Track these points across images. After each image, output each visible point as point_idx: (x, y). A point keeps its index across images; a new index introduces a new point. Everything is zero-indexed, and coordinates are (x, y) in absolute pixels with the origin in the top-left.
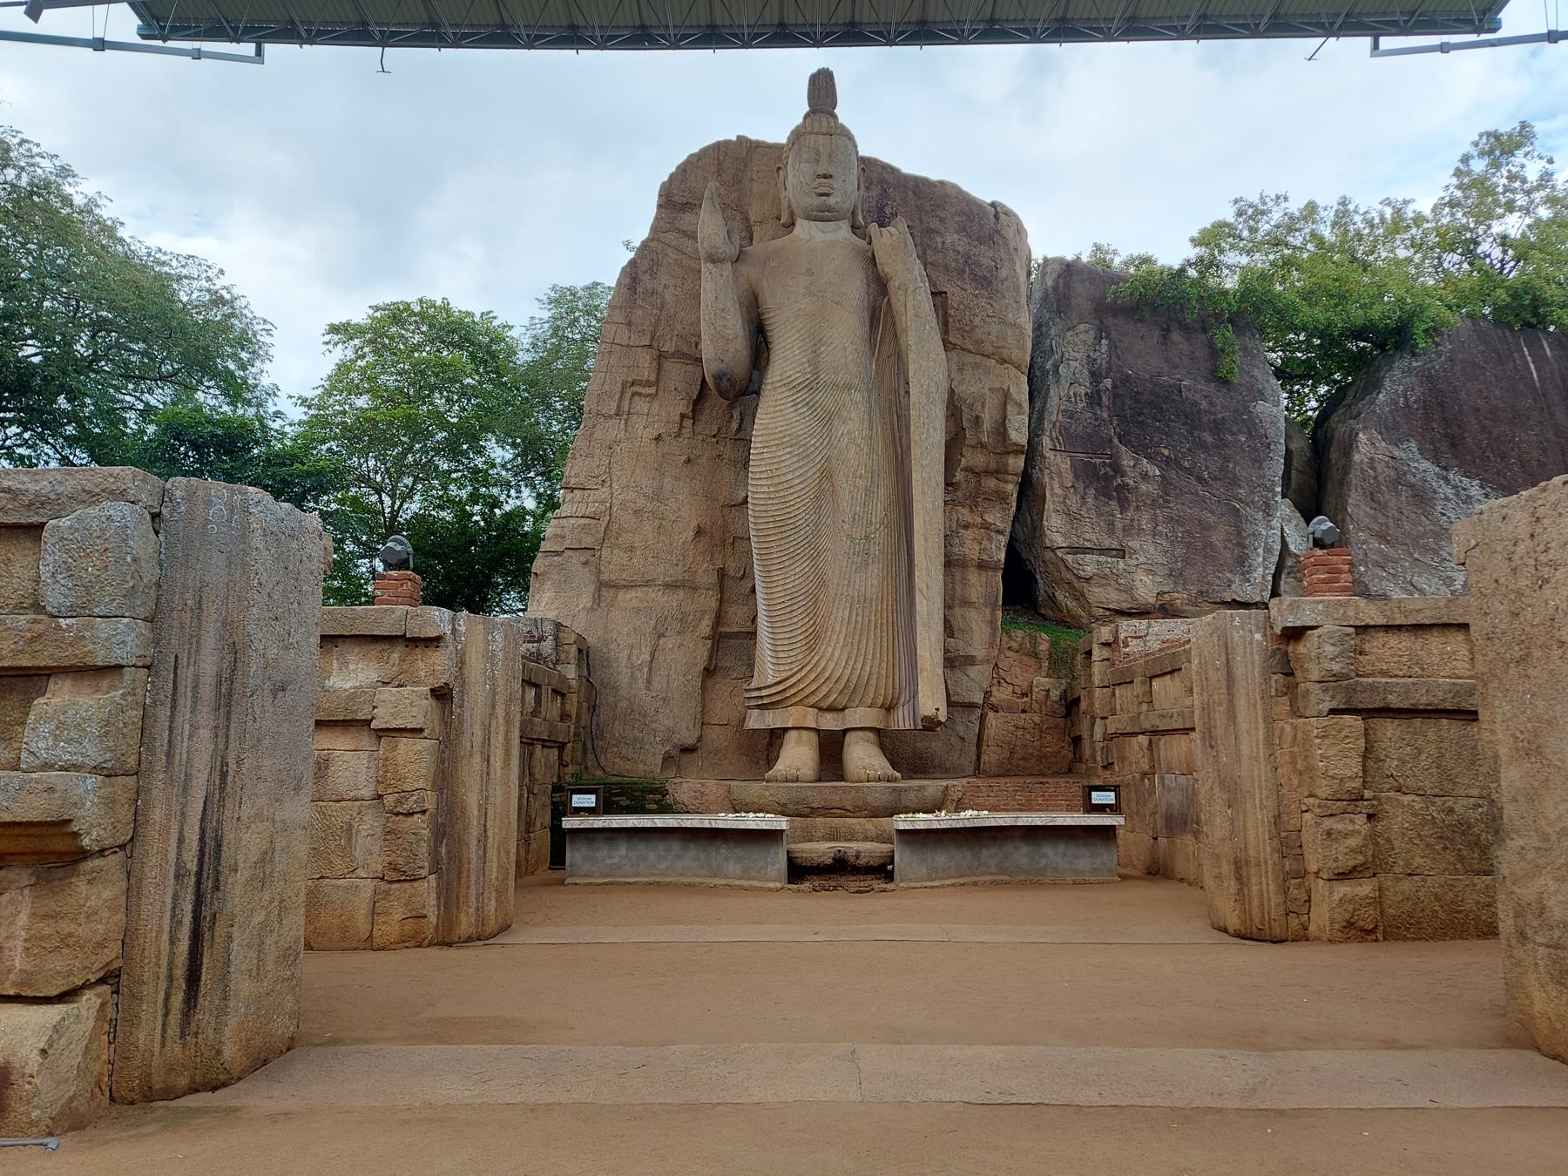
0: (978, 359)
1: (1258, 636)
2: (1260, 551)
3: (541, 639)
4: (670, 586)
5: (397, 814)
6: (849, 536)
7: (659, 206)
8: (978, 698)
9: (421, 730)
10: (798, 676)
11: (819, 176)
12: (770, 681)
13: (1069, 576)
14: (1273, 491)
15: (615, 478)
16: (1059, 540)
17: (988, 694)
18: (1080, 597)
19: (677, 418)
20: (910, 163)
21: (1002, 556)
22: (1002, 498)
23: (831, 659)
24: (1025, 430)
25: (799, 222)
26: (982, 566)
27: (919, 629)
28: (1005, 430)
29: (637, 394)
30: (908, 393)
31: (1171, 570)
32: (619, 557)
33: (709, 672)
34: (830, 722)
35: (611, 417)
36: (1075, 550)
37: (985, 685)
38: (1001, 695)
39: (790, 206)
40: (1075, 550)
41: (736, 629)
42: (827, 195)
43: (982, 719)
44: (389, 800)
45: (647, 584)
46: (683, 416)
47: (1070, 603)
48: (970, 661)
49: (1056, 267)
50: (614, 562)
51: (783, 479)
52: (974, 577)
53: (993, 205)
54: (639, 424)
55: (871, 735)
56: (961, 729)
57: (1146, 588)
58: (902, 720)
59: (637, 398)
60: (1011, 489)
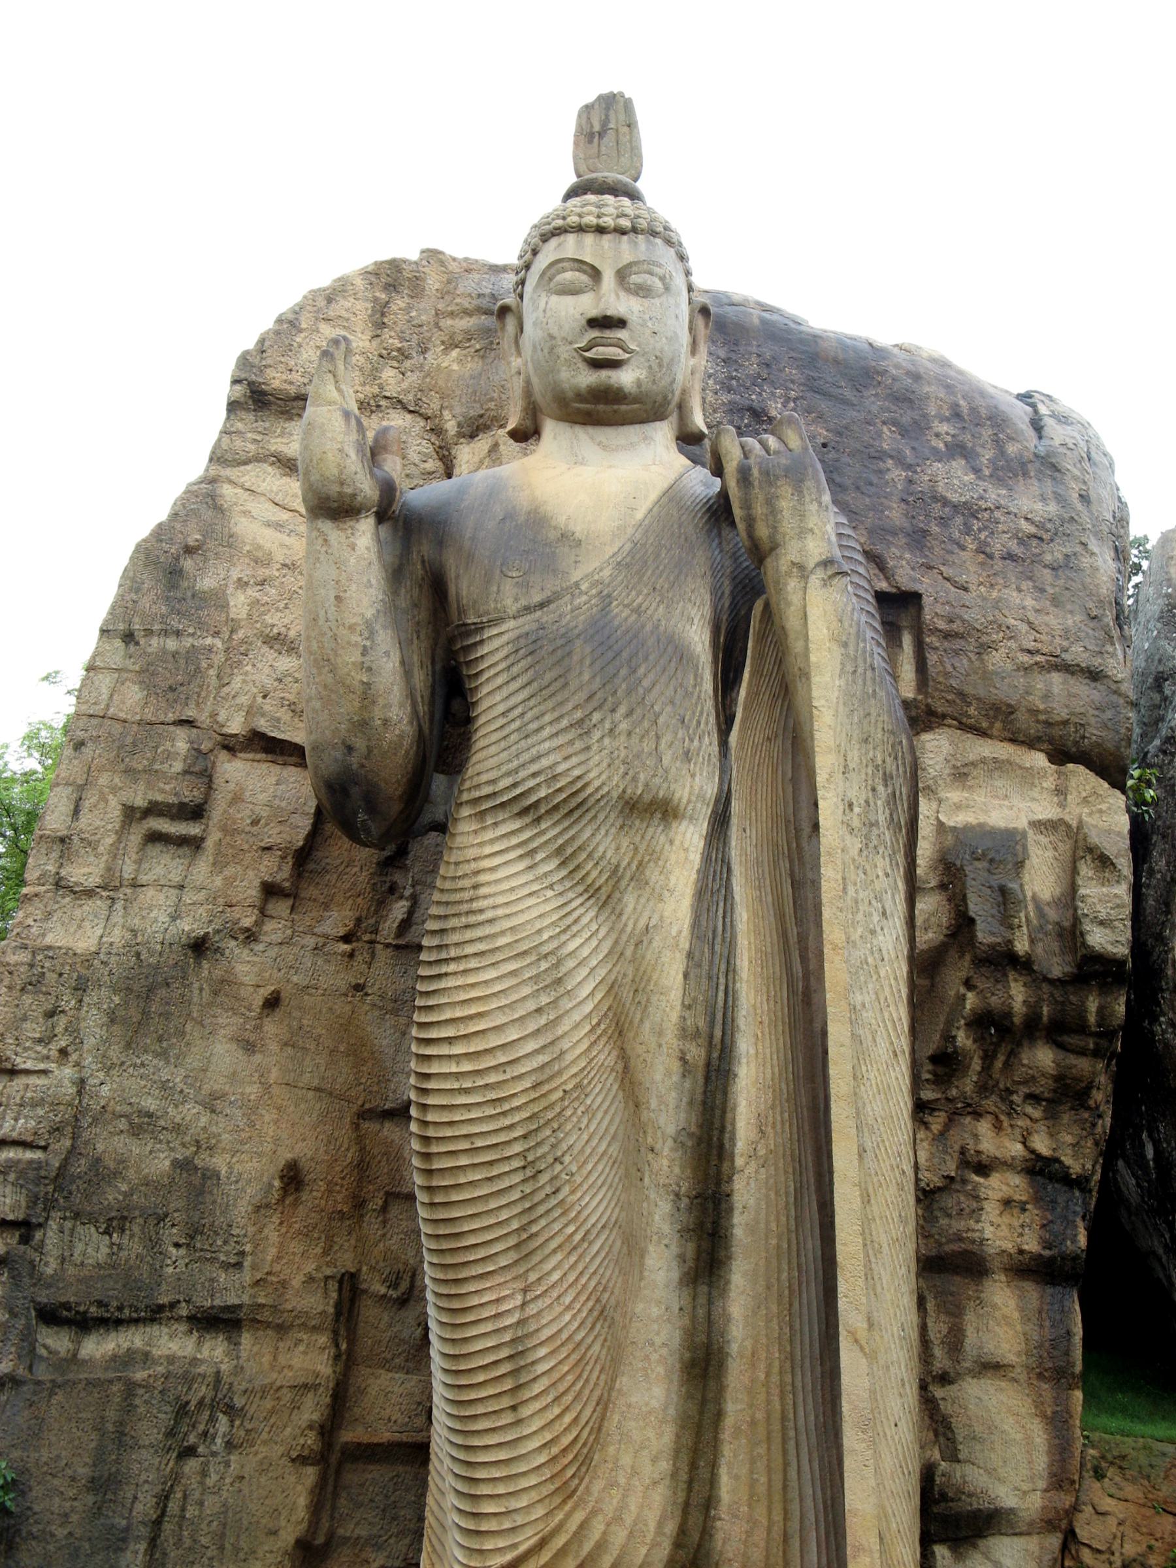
7: (233, 406)
11: (593, 323)
20: (834, 303)
21: (1082, 1240)
25: (550, 428)
27: (852, 1439)
28: (1076, 921)
29: (155, 838)
30: (816, 827)
35: (90, 893)
39: (528, 393)
41: (385, 1435)
42: (614, 364)
46: (270, 890)
51: (494, 1041)
59: (155, 850)
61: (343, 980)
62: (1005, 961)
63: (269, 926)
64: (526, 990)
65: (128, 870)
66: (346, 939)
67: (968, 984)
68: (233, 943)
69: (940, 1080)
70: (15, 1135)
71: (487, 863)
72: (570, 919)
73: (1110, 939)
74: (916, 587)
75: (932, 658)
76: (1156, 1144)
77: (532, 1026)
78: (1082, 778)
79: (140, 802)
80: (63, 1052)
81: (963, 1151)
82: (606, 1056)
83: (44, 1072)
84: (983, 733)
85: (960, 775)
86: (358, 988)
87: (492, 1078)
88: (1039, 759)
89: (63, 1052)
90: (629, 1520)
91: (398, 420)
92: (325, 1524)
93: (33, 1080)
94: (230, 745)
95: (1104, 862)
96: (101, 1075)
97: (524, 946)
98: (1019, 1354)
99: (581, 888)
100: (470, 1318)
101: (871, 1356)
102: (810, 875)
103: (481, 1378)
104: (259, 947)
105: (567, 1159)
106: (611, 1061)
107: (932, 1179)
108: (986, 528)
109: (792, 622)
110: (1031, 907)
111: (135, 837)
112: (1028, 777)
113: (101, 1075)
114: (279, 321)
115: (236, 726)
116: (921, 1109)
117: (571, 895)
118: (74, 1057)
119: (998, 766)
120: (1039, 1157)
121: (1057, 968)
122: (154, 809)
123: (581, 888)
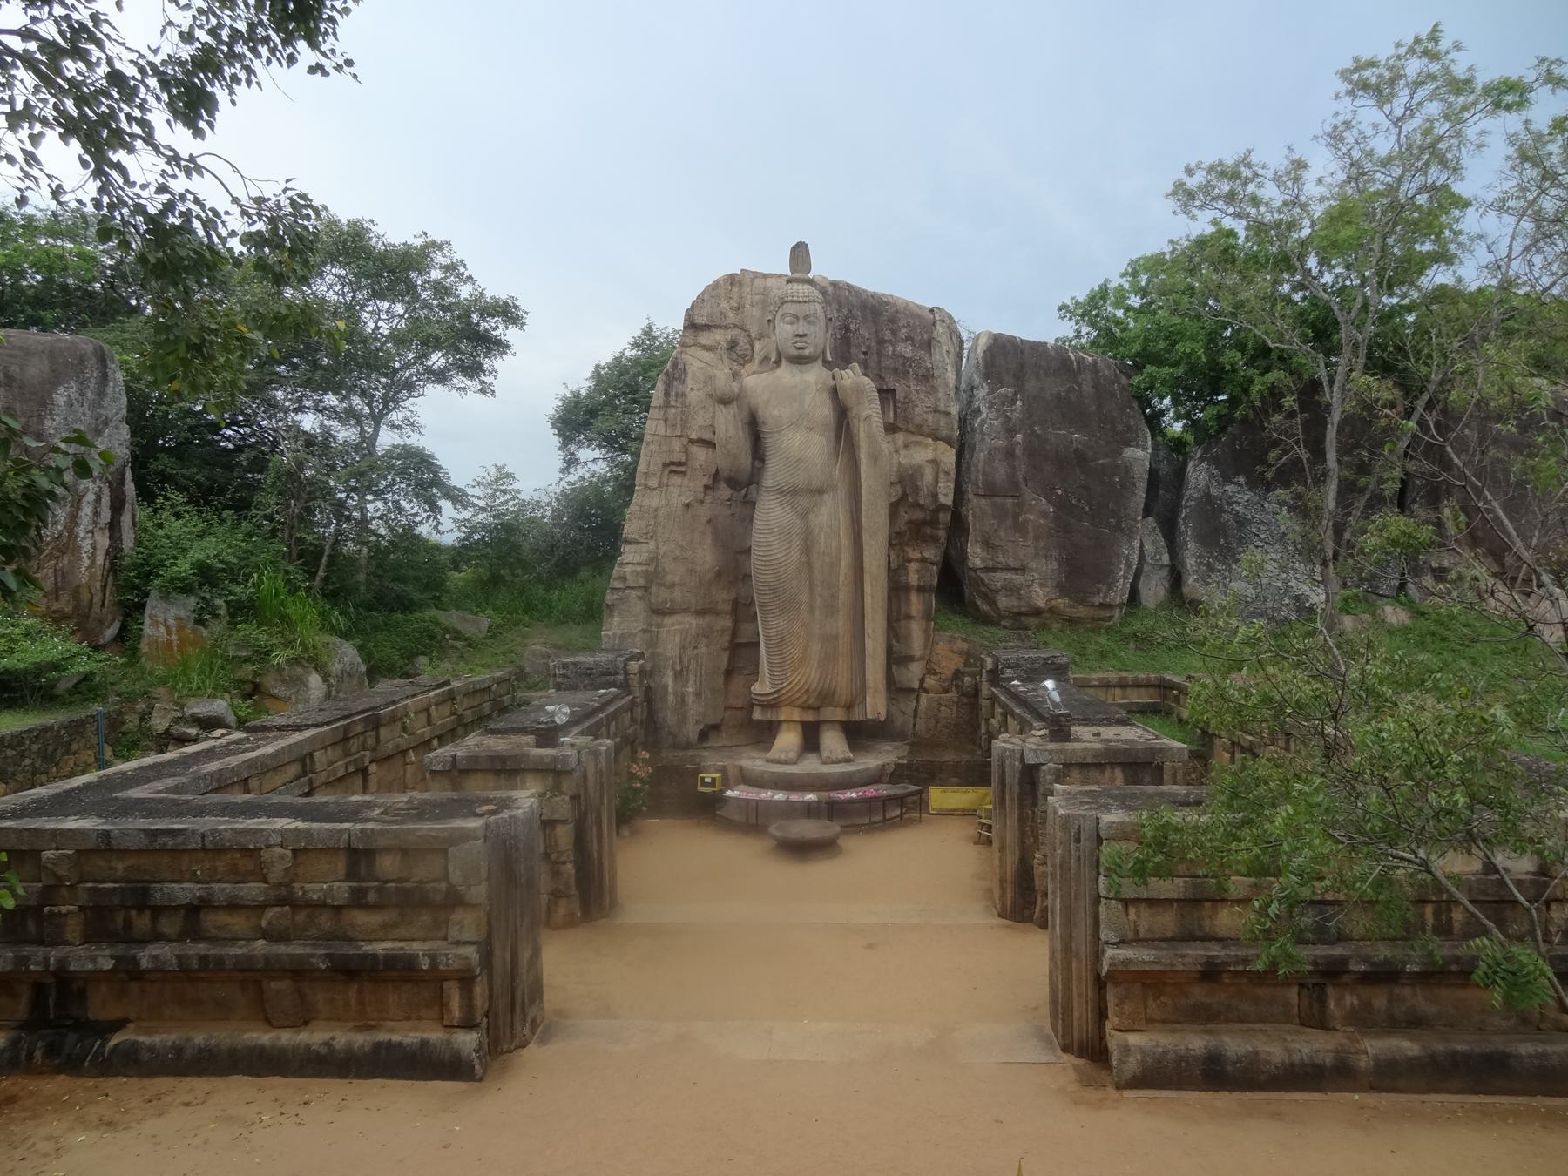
0: (920, 438)
3: (617, 673)
4: (700, 613)
8: (916, 685)
12: (768, 690)
14: (1135, 520)
16: (978, 562)
17: (922, 681)
18: (993, 603)
26: (920, 589)
29: (672, 471)
32: (664, 593)
33: (729, 673)
34: (810, 717)
36: (988, 570)
38: (930, 682)
40: (988, 570)
44: (553, 856)
45: (684, 611)
46: (706, 487)
47: (986, 608)
48: (911, 659)
49: (983, 343)
50: (660, 595)
53: (932, 310)
54: (675, 491)
55: (837, 726)
57: (1040, 597)
58: (857, 716)
60: (942, 533)
61: (729, 512)
62: (917, 505)
69: (897, 541)
78: (942, 445)
85: (906, 446)
88: (930, 440)
91: (736, 332)
95: (947, 474)
112: (926, 446)
115: (694, 436)
116: (891, 545)
119: (918, 443)
122: (672, 463)
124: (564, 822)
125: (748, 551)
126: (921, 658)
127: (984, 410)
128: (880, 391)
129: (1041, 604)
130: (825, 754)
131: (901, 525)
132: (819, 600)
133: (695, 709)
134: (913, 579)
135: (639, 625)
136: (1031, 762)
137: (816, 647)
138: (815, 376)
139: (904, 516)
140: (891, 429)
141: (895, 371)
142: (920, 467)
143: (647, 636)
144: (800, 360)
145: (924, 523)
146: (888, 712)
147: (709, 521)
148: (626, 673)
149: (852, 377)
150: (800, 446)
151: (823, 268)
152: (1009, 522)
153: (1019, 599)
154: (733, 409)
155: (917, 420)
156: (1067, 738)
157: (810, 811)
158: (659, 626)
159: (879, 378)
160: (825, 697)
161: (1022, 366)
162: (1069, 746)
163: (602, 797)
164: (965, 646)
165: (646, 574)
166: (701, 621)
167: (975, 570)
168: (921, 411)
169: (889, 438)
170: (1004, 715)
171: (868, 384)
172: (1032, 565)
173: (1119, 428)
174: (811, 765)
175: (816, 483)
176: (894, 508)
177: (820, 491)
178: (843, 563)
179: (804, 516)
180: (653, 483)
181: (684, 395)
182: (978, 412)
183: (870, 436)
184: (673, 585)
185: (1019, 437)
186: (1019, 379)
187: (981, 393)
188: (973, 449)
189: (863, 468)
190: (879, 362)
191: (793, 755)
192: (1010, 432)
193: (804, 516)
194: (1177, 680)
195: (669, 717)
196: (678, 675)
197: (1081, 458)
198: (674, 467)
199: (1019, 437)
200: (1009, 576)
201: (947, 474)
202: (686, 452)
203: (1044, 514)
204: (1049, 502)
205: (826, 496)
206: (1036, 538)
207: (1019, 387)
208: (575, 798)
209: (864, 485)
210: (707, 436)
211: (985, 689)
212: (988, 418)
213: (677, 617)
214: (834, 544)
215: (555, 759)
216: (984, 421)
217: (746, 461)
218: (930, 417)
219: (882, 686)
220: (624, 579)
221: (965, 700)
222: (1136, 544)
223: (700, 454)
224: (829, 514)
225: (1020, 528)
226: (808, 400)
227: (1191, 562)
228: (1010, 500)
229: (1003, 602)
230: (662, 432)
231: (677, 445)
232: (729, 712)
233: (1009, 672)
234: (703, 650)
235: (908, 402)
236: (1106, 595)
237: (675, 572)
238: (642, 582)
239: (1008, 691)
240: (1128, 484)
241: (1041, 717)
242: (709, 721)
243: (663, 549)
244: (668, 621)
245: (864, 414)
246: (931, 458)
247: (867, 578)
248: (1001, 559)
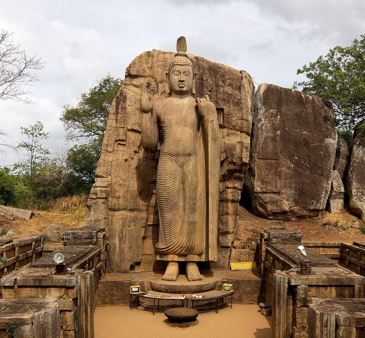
0: (234, 131)
1: (286, 285)
2: (324, 192)
3: (92, 238)
4: (132, 210)
5: (66, 331)
6: (189, 203)
8: (230, 245)
9: (71, 310)
10: (172, 246)
13: (261, 202)
15: (113, 173)
17: (233, 243)
18: (265, 208)
19: (133, 153)
21: (240, 197)
22: (240, 179)
23: (182, 241)
24: (248, 159)
26: (233, 201)
28: (242, 158)
29: (119, 144)
31: (295, 199)
32: (115, 201)
34: (182, 259)
35: (111, 152)
37: (232, 241)
38: (236, 243)
43: (231, 251)
44: (64, 327)
45: (124, 209)
46: (135, 152)
47: (262, 210)
50: (112, 201)
52: (230, 205)
56: (224, 255)
57: (286, 206)
59: (119, 146)
61: (145, 164)
63: (135, 157)
64: (171, 179)
65: (116, 148)
66: (146, 158)
67: (227, 166)
68: (131, 159)
69: (224, 178)
70: (104, 186)
71: (166, 161)
72: (177, 170)
73: (246, 160)
74: (224, 108)
75: (225, 118)
76: (251, 180)
77: (172, 183)
79: (117, 139)
80: (109, 174)
81: (226, 186)
82: (181, 186)
83: (107, 177)
84: (231, 129)
86: (147, 165)
87: (167, 190)
89: (109, 174)
90: (183, 241)
92: (146, 234)
93: (105, 178)
94: (129, 130)
96: (114, 178)
97: (171, 173)
98: (231, 212)
99: (178, 165)
100: (165, 218)
101: (213, 224)
102: (207, 159)
103: (166, 225)
104: (134, 160)
105: (176, 199)
106: (182, 187)
107: (221, 190)
108: (234, 98)
109: (206, 127)
110: (236, 155)
111: (116, 144)
112: (237, 135)
113: (114, 178)
114: (132, 62)
115: (129, 128)
117: (177, 166)
118: (111, 175)
119: (233, 134)
120: (235, 187)
121: (240, 163)
122: (119, 140)
123: (178, 165)
124: (70, 311)
125: (155, 182)
126: (233, 233)
127: (263, 119)
128: (217, 109)
129: (287, 209)
130: (189, 277)
131: (224, 171)
132: (188, 205)
133: (128, 255)
134: (230, 197)
135: (101, 216)
136: (293, 284)
137: (186, 227)
138: (188, 101)
139: (226, 167)
140: (221, 127)
141: (224, 99)
142: (234, 145)
143: (106, 220)
144: (181, 94)
145: (235, 171)
146: (218, 259)
147: (136, 168)
148: (97, 238)
149: (205, 102)
150: (181, 133)
151: (192, 51)
152: (273, 171)
153: (277, 206)
154: (149, 115)
155: (234, 123)
156: (310, 273)
157: (182, 304)
158: (112, 216)
159: (216, 103)
160: (190, 250)
161: (280, 100)
162: (311, 277)
163: (88, 299)
164: (252, 228)
165: (106, 192)
166: (132, 214)
167: (257, 193)
168: (235, 120)
169: (221, 130)
170: (274, 260)
171: (212, 105)
172: (283, 191)
173: (324, 129)
174: (182, 282)
175: (188, 151)
176: (222, 163)
177: (189, 155)
178: (199, 188)
179: (182, 166)
180: (110, 149)
181: (125, 108)
182: (261, 120)
183: (213, 130)
184: (119, 197)
185: (279, 132)
186: (279, 106)
187: (262, 112)
188: (258, 138)
189: (210, 144)
190: (217, 95)
191: (174, 277)
192: (275, 129)
193: (182, 166)
194: (348, 244)
195: (116, 258)
196: (121, 239)
197: (306, 143)
198: (120, 142)
199: (279, 132)
200: (273, 196)
201: (247, 148)
202: (126, 135)
203: (289, 168)
204: (292, 162)
205: (192, 157)
206: (285, 179)
207: (279, 110)
208: (75, 300)
209: (210, 152)
210: (136, 128)
211: (264, 248)
212: (264, 123)
213: (121, 212)
214: (195, 180)
215: (66, 281)
216: (262, 125)
217: (154, 139)
218: (239, 122)
219: (216, 246)
220: (96, 194)
221: (253, 252)
222: (330, 182)
223: (133, 136)
224: (194, 166)
225: (279, 174)
226: (184, 112)
227: (354, 191)
228: (274, 161)
229: (270, 207)
230: (115, 125)
231: (121, 131)
232: (144, 256)
233: (274, 240)
234: (132, 227)
235: (229, 114)
236: (316, 205)
237: (121, 192)
238: (104, 196)
239: (274, 249)
240: (327, 155)
241: (295, 263)
242: (135, 260)
243: (114, 180)
244: (116, 213)
245: (211, 119)
246: (238, 140)
247: (210, 195)
248: (269, 188)
